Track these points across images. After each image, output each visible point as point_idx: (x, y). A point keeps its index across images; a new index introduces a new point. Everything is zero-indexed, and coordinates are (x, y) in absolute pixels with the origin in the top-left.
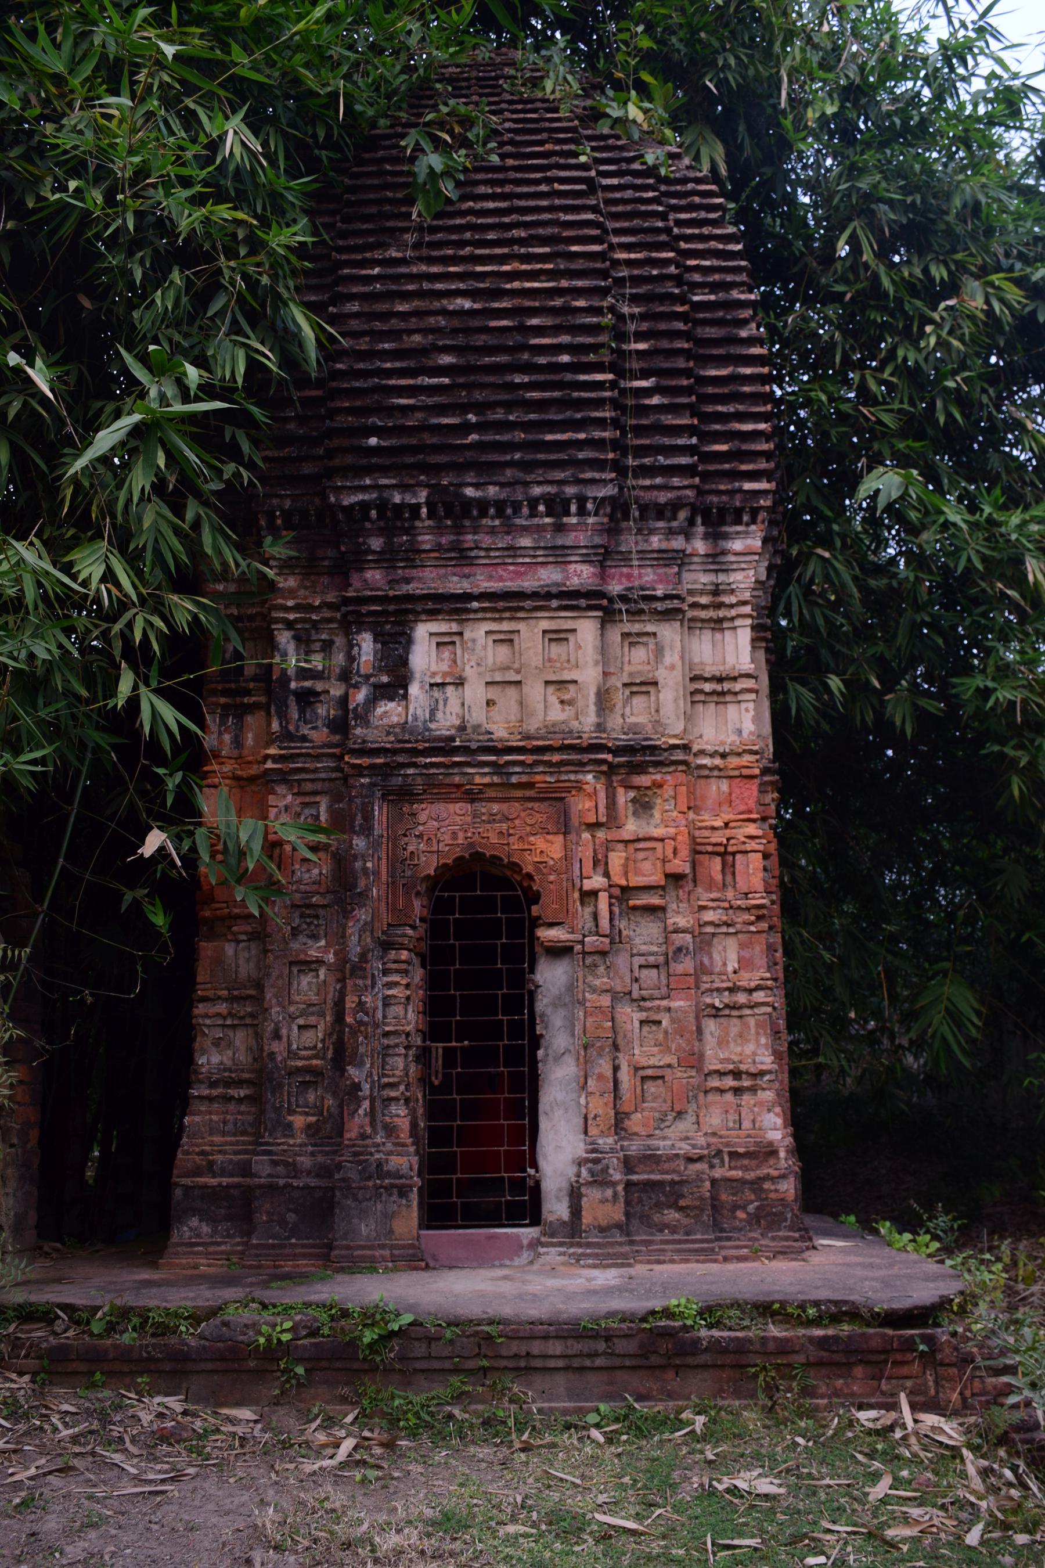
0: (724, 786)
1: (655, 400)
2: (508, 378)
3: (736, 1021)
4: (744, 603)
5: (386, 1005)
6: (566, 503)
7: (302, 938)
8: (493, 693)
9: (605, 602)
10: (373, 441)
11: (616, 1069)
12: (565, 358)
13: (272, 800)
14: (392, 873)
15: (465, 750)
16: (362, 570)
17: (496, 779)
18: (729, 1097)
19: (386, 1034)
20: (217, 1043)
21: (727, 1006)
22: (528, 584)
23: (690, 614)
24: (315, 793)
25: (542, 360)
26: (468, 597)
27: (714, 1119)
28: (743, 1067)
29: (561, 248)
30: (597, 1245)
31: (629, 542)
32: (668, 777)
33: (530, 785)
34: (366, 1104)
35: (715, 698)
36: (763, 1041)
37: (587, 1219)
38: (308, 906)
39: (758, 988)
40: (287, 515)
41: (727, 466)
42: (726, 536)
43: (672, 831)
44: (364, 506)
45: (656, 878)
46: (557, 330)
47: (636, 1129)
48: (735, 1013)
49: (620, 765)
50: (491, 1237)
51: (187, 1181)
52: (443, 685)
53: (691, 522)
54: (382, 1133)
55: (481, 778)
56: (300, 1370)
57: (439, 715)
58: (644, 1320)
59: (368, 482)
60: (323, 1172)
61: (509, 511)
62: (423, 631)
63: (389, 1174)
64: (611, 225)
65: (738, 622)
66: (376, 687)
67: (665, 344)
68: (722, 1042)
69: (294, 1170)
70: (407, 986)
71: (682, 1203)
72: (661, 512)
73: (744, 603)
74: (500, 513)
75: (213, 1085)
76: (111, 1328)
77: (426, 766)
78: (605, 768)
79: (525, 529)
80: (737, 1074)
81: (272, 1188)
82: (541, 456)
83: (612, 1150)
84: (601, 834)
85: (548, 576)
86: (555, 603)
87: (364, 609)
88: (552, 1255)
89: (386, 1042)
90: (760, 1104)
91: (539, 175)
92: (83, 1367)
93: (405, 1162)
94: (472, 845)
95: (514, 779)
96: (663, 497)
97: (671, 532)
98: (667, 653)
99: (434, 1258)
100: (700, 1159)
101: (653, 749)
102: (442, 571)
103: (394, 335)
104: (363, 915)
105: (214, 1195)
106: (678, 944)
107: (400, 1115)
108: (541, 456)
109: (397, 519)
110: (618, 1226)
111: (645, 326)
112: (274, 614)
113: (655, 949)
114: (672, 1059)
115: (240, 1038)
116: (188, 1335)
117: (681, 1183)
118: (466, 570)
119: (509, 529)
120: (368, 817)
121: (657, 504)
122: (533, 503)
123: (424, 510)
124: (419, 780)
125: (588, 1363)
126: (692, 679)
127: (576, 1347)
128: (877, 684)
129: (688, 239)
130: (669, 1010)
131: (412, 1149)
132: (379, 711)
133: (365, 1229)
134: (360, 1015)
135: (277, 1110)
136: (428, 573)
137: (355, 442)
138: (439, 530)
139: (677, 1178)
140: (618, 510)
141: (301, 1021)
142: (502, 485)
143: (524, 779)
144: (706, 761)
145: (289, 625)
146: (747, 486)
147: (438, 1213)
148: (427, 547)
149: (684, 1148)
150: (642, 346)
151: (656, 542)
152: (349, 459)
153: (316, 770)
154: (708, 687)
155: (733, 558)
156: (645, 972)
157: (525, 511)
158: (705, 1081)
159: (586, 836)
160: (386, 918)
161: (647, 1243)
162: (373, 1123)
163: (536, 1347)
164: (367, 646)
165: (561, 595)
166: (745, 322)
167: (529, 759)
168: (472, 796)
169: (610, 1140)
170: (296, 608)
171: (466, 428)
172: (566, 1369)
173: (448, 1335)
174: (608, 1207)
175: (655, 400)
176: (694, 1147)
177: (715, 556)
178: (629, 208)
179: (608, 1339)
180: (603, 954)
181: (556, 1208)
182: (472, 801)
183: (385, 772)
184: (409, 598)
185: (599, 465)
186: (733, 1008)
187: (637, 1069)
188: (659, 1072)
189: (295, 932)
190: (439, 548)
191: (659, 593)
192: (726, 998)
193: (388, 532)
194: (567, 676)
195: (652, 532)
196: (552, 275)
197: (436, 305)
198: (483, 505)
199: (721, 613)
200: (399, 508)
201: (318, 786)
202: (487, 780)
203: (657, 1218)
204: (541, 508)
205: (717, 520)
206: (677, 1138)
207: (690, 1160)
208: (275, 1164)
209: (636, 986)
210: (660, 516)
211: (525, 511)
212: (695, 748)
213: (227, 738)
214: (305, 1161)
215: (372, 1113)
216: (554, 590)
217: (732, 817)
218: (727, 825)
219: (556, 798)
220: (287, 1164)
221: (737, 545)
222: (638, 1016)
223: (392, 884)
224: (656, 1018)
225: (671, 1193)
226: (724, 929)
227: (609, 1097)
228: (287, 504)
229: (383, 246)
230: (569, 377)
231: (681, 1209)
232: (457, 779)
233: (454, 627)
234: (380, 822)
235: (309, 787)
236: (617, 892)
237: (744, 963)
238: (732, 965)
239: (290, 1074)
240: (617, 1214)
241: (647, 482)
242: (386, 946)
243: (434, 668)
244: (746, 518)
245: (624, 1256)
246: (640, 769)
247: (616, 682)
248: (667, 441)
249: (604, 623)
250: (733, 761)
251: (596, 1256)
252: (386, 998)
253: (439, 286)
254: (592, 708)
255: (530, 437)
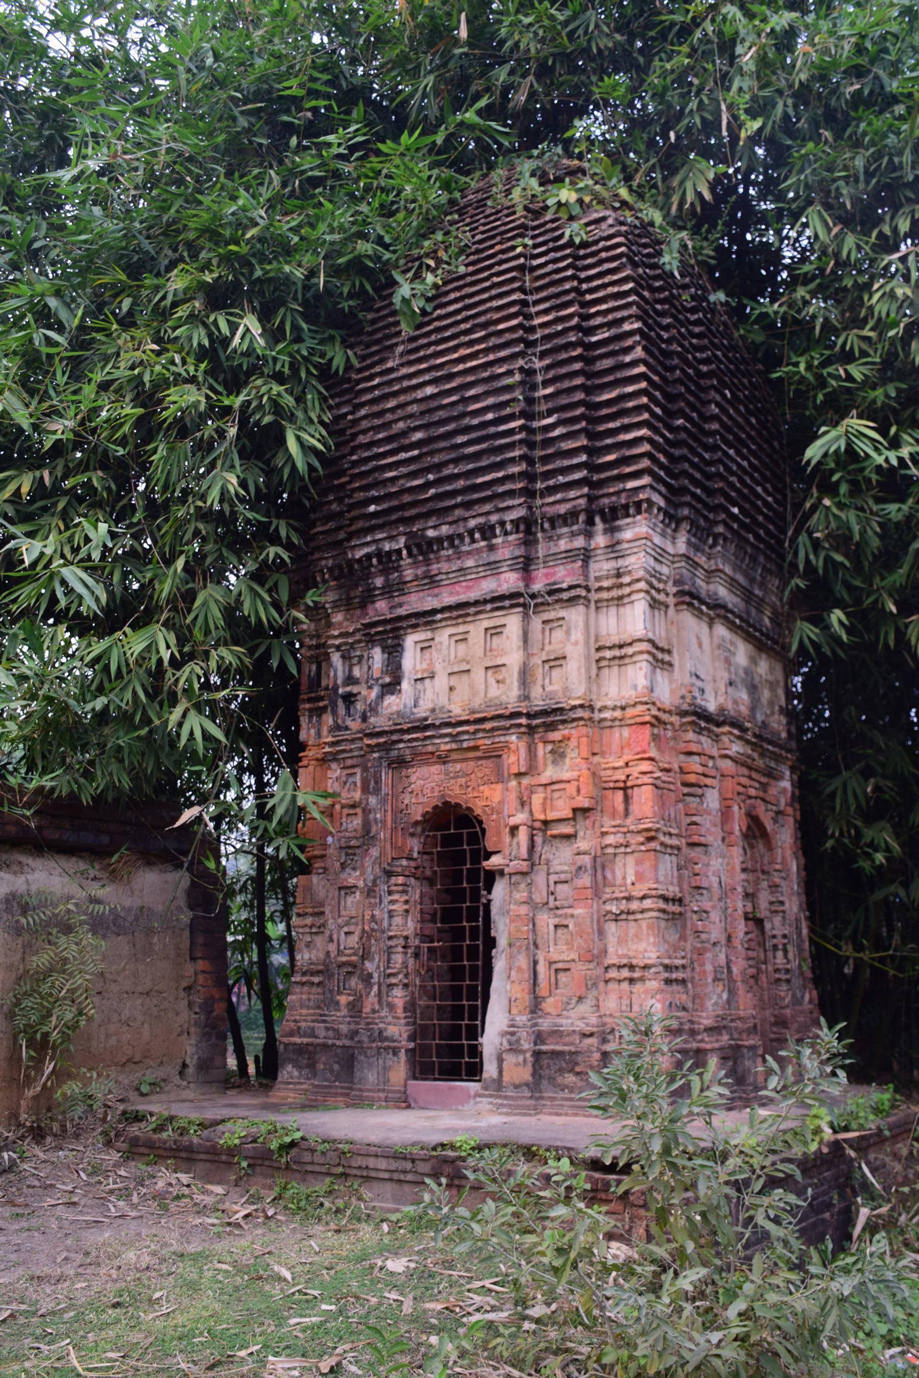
0: (626, 732)
1: (557, 432)
2: (454, 441)
3: (632, 924)
4: (638, 580)
5: (391, 917)
6: (492, 528)
7: (348, 870)
8: (454, 681)
9: (521, 600)
10: (372, 508)
11: (535, 963)
12: (490, 416)
13: (329, 774)
14: (394, 822)
15: (433, 726)
16: (373, 602)
17: (454, 746)
18: (625, 985)
19: (390, 938)
20: (308, 945)
21: (622, 912)
22: (473, 595)
23: (594, 596)
24: (353, 766)
25: (475, 422)
26: (434, 612)
27: (611, 1004)
28: (634, 962)
29: (492, 329)
30: (512, 1098)
31: (541, 550)
32: (573, 731)
33: (476, 748)
34: (375, 988)
35: (617, 662)
36: (652, 940)
37: (506, 1078)
38: (350, 847)
39: (644, 898)
40: (331, 570)
41: (616, 472)
42: (618, 529)
43: (575, 774)
44: (369, 556)
45: (567, 813)
46: (487, 394)
47: (549, 1010)
48: (631, 917)
49: (537, 726)
50: (451, 1088)
51: (285, 1040)
52: (422, 679)
53: (590, 522)
54: (386, 1009)
55: (445, 745)
56: (244, 1164)
57: (421, 702)
58: (434, 1149)
59: (369, 539)
60: (353, 1034)
61: (457, 542)
62: (411, 641)
63: (386, 1039)
64: (531, 298)
65: (634, 597)
66: (383, 686)
67: (566, 384)
68: (621, 941)
69: (338, 1035)
70: (407, 902)
71: (577, 1069)
72: (569, 518)
73: (638, 580)
74: (452, 545)
75: (304, 974)
76: (160, 1128)
77: (409, 741)
78: (523, 730)
79: (469, 553)
80: (632, 967)
81: (325, 1046)
82: (476, 496)
83: (524, 1026)
84: (525, 781)
85: (488, 586)
86: (489, 607)
87: (373, 631)
88: (484, 1103)
89: (390, 943)
90: (646, 991)
91: (486, 274)
92: (145, 1151)
93: (397, 1029)
94: (443, 796)
95: (465, 745)
96: (563, 509)
97: (573, 535)
98: (573, 632)
99: (415, 1101)
100: (591, 1035)
101: (561, 710)
102: (421, 594)
103: (387, 425)
104: (374, 852)
105: (300, 1050)
106: (579, 864)
107: (399, 997)
108: (476, 496)
109: (389, 562)
110: (527, 1085)
111: (551, 374)
112: (330, 642)
113: (566, 868)
114: (574, 955)
115: (319, 940)
116: (194, 1138)
117: (576, 1053)
118: (436, 591)
119: (459, 555)
120: (378, 781)
121: (559, 516)
122: (471, 533)
123: (405, 552)
124: (407, 752)
125: (402, 1177)
126: (598, 649)
127: (394, 1165)
128: (894, 610)
129: (591, 291)
130: (572, 916)
131: (403, 1021)
132: (386, 703)
133: (371, 1077)
134: (374, 925)
135: (331, 991)
136: (413, 598)
137: (363, 511)
138: (415, 564)
139: (573, 1049)
140: (527, 528)
141: (346, 929)
142: (450, 523)
143: (472, 743)
144: (607, 715)
145: (338, 648)
146: (631, 485)
147: (422, 1069)
148: (409, 579)
149: (580, 1026)
150: (549, 390)
151: (563, 545)
152: (361, 524)
153: (351, 750)
154: (608, 654)
155: (625, 546)
156: (559, 886)
157: (467, 540)
158: (602, 971)
159: (513, 783)
160: (390, 853)
161: (552, 1099)
162: (380, 1002)
163: (372, 1162)
164: (378, 656)
165: (494, 600)
166: (630, 349)
167: (471, 728)
168: (443, 760)
169: (524, 1018)
170: (341, 635)
171: (428, 485)
172: (391, 1180)
173: (321, 1148)
174: (520, 1069)
175: (557, 432)
176: (587, 1025)
177: (612, 546)
178: (547, 280)
179: (413, 1161)
180: (524, 874)
181: (490, 1069)
182: (444, 763)
183: (386, 748)
184: (400, 618)
185: (511, 494)
186: (628, 913)
187: (551, 963)
188: (566, 966)
189: (343, 866)
190: (417, 578)
191: (564, 586)
192: (623, 905)
193: (385, 572)
194: (499, 662)
195: (559, 537)
196: (487, 351)
197: (408, 397)
198: (439, 540)
199: (620, 592)
200: (389, 553)
201: (354, 762)
202: (448, 747)
203: (559, 1080)
204: (477, 536)
205: (613, 516)
206: (579, 1019)
207: (585, 1035)
208: (327, 1029)
209: (551, 898)
210: (565, 524)
211: (467, 540)
212: (598, 705)
213: (312, 731)
214: (344, 1028)
215: (379, 994)
216: (488, 597)
217: (631, 757)
218: (627, 764)
219: (494, 755)
220: (334, 1030)
221: (628, 535)
222: (553, 922)
223: (394, 830)
224: (565, 922)
225: (569, 1061)
226: (622, 850)
227: (526, 986)
228: (330, 563)
229: (383, 361)
230: (492, 430)
231: (578, 1074)
232: (430, 749)
233: (429, 635)
234: (387, 785)
235: (349, 762)
236: (538, 825)
237: (640, 876)
238: (630, 878)
239: (339, 967)
240: (525, 1074)
241: (551, 499)
242: (389, 874)
243: (418, 667)
244: (631, 511)
245: (528, 1107)
246: (551, 727)
247: (537, 660)
248: (566, 463)
249: (526, 616)
250: (630, 712)
251: (510, 1106)
252: (390, 911)
253: (414, 382)
254: (516, 684)
255: (468, 483)
